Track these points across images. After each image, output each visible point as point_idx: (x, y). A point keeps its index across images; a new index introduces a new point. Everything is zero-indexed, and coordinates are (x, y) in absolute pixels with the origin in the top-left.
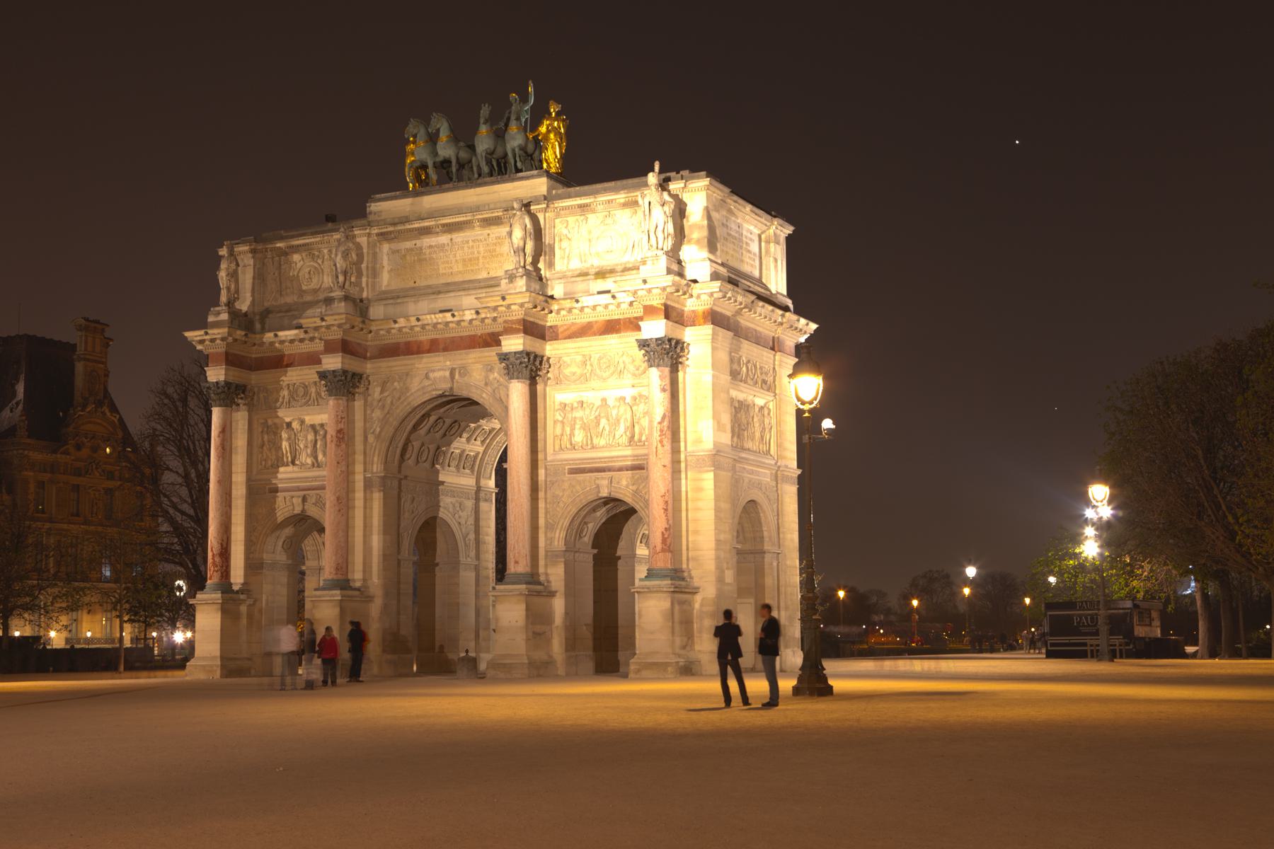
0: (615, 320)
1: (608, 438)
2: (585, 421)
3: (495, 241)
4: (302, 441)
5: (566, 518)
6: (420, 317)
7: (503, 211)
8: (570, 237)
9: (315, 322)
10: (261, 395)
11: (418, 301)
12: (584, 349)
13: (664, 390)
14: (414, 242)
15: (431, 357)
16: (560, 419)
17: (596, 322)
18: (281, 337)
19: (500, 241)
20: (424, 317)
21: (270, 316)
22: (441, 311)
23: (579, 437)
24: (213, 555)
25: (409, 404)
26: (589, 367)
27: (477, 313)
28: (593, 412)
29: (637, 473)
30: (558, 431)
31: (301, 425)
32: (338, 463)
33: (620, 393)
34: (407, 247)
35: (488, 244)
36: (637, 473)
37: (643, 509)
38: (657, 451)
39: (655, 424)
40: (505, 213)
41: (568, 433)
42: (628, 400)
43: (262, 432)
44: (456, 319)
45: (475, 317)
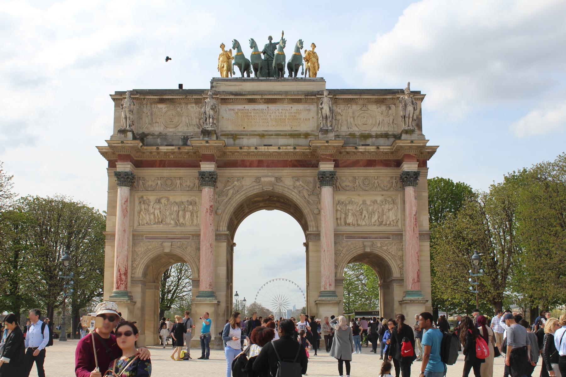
0: (373, 160)
1: (367, 221)
2: (354, 212)
4: (168, 210)
5: (344, 262)
6: (258, 147)
8: (342, 114)
10: (141, 182)
12: (354, 174)
13: (416, 198)
14: (244, 106)
15: (259, 170)
16: (340, 209)
17: (362, 160)
18: (161, 149)
20: (260, 147)
21: (148, 137)
22: (265, 145)
23: (350, 220)
24: (120, 274)
25: (244, 194)
26: (357, 183)
27: (295, 148)
28: (358, 207)
29: (386, 241)
30: (339, 217)
31: (168, 201)
32: (211, 224)
33: (374, 198)
36: (386, 241)
37: (390, 260)
38: (414, 230)
39: (413, 216)
40: (306, 97)
41: (344, 217)
42: (378, 202)
43: (140, 202)
44: (281, 150)
45: (292, 150)
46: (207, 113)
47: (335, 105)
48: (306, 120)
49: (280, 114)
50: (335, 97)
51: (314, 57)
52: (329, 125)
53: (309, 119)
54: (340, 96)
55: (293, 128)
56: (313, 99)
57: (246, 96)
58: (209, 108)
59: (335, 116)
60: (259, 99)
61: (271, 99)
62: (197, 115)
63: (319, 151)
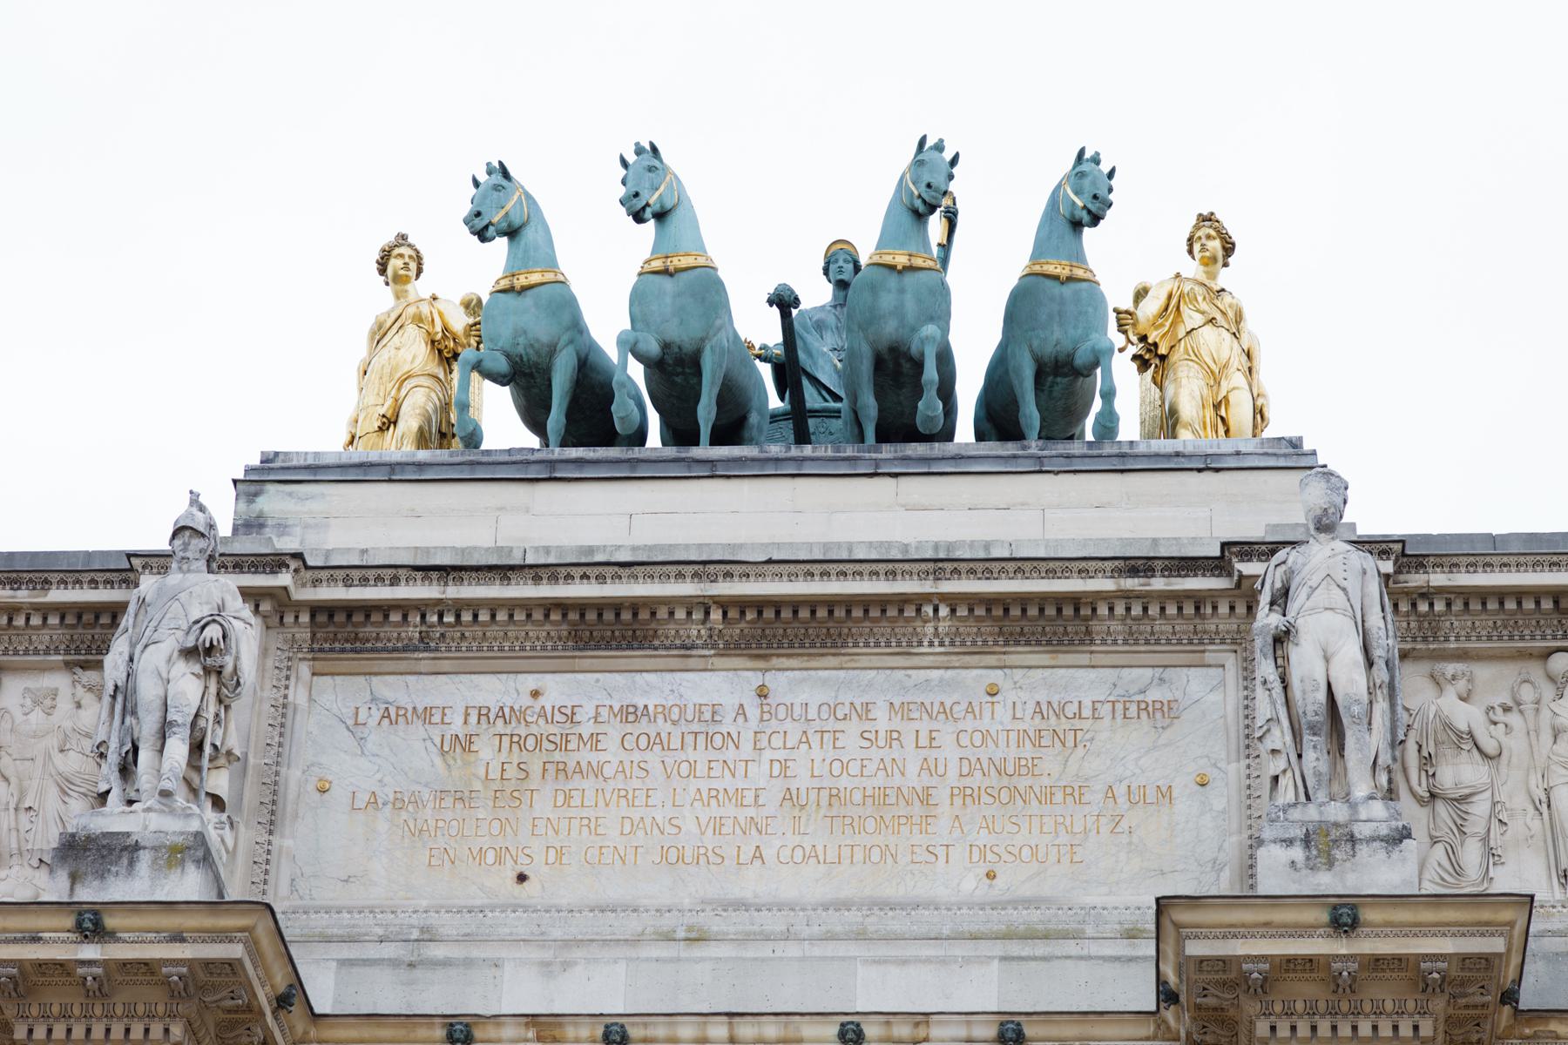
3: (1030, 724)
7: (1118, 573)
9: (35, 939)
11: (567, 965)
14: (530, 682)
19: (1065, 724)
34: (480, 700)
35: (986, 734)
40: (1131, 584)
46: (148, 691)
47: (1424, 667)
48: (1137, 797)
49: (875, 754)
50: (1416, 580)
51: (1212, 321)
52: (1361, 789)
53: (1166, 794)
54: (1472, 567)
55: (999, 869)
56: (1198, 600)
57: (554, 579)
58: (169, 644)
59: (1427, 760)
60: (680, 614)
61: (795, 604)
62: (75, 762)
63: (1262, 1028)
